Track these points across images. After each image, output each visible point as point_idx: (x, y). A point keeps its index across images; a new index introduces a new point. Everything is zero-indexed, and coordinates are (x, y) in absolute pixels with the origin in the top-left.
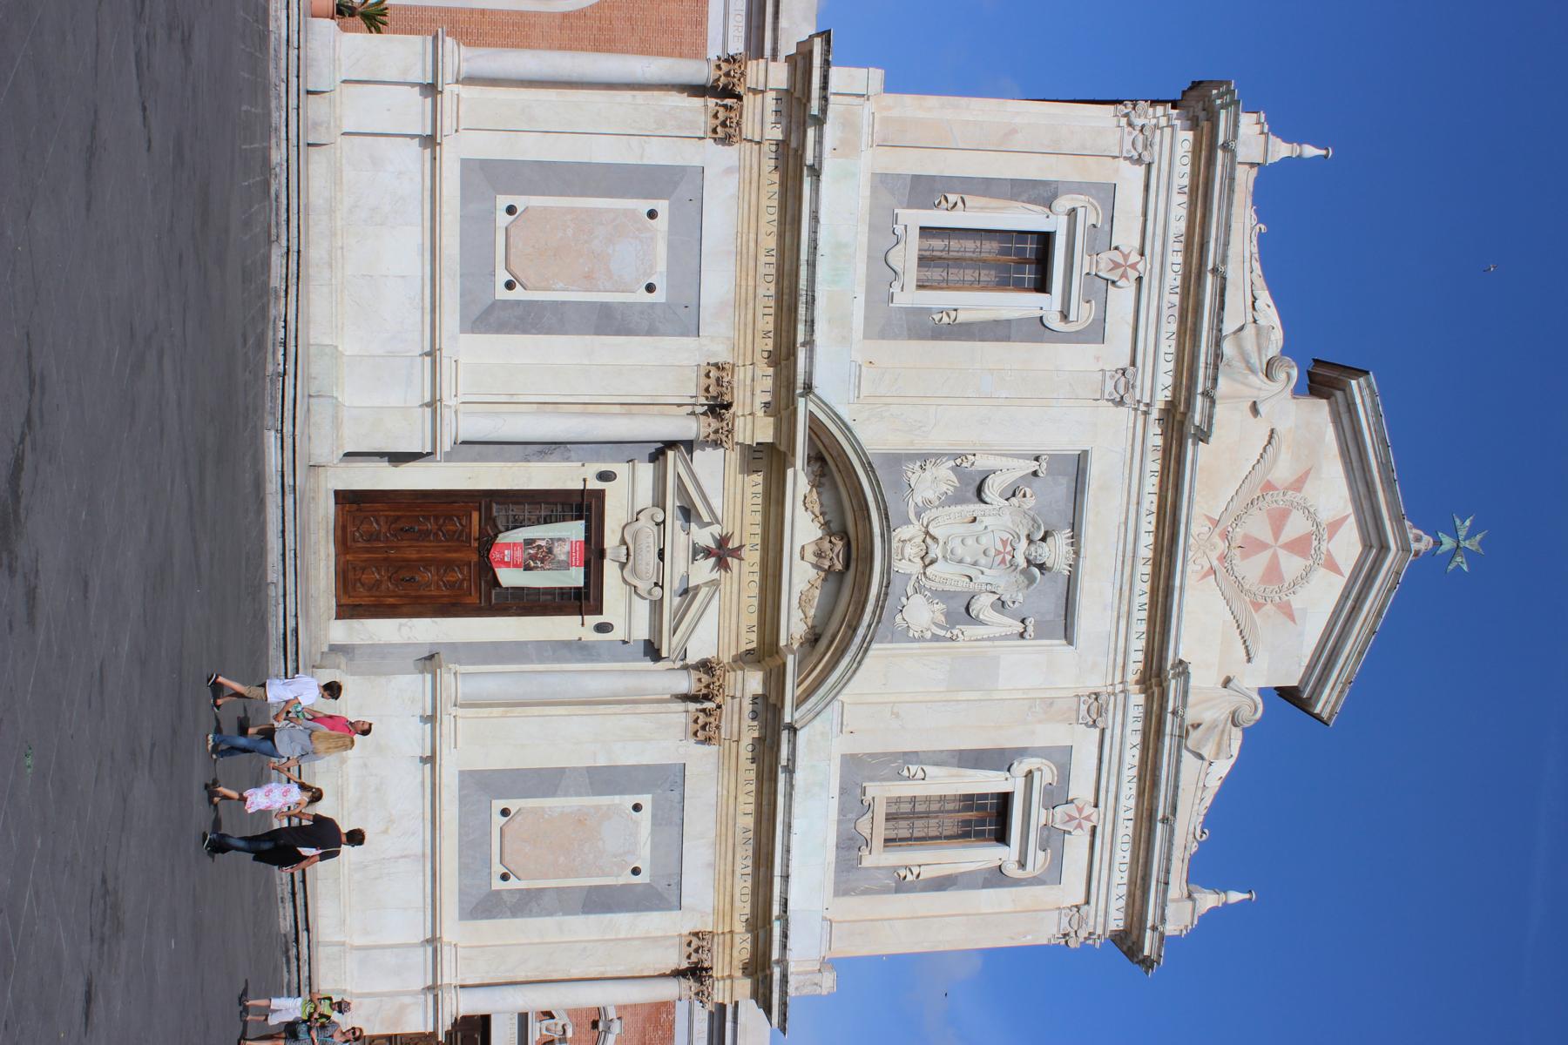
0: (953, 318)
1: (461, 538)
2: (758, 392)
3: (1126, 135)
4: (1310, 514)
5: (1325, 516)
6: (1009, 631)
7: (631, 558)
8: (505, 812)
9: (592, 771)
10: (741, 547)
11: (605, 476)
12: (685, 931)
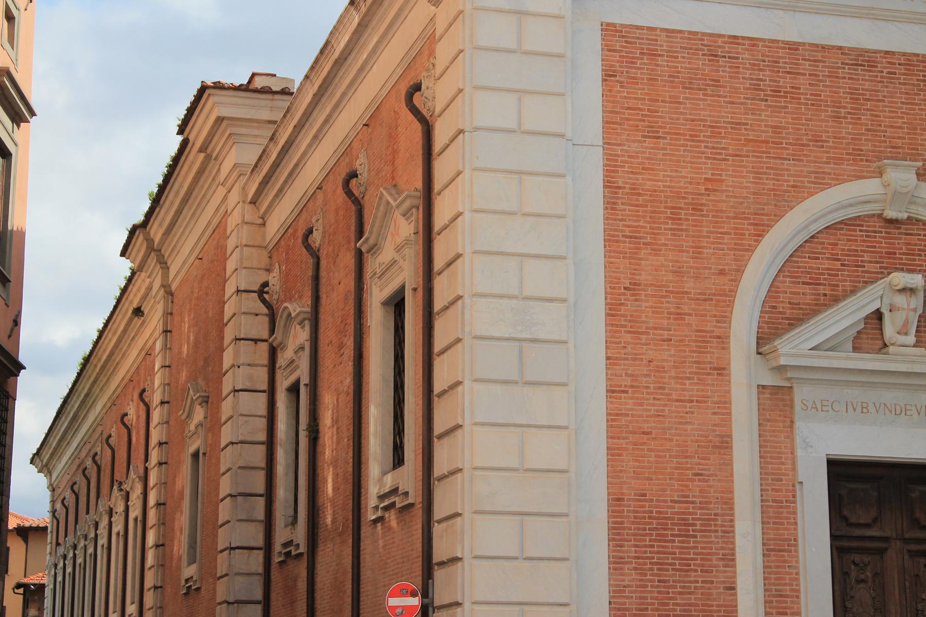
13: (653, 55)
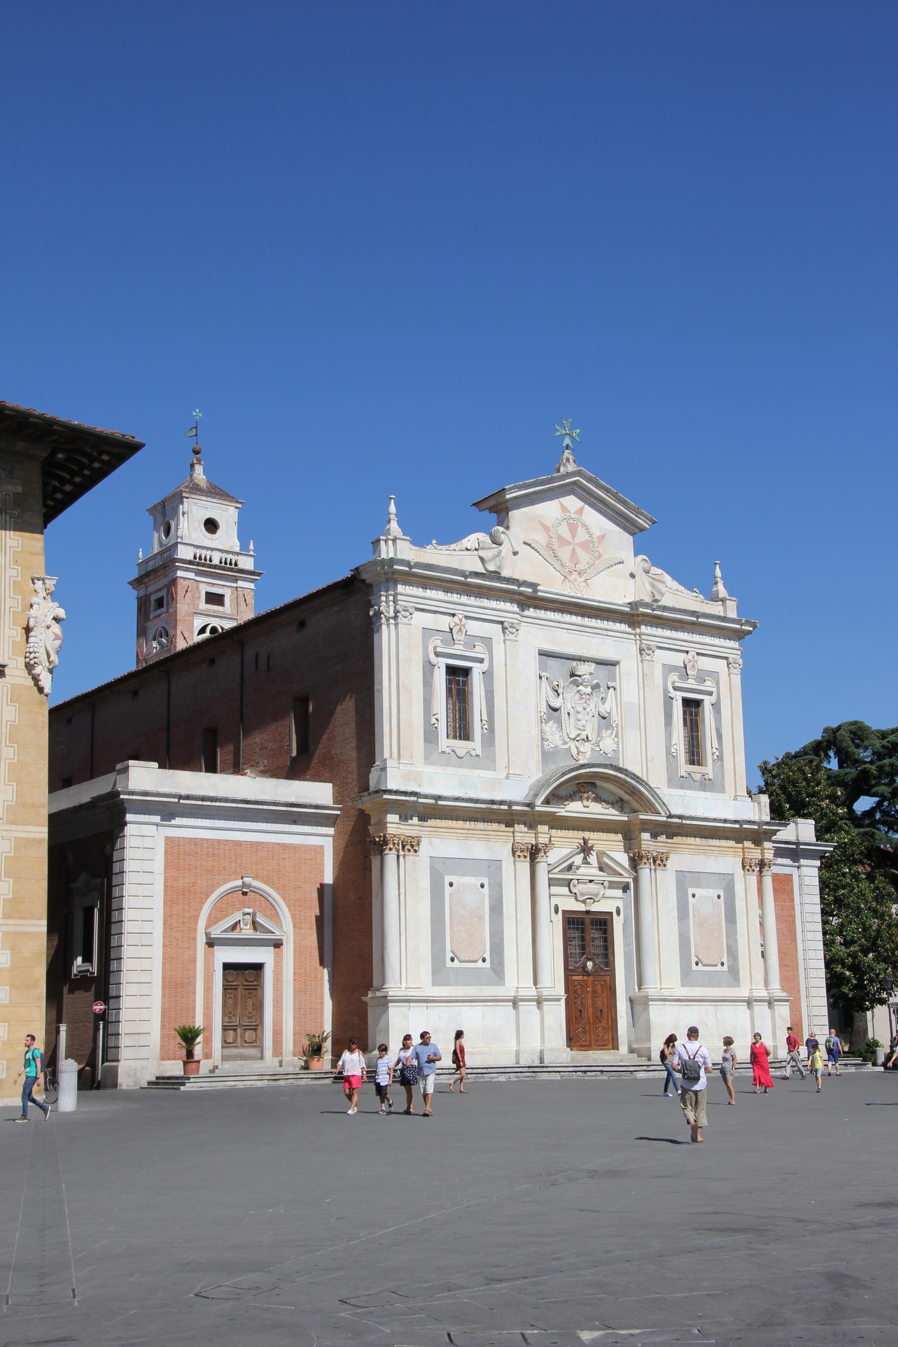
0: (486, 723)
1: (584, 984)
5: (559, 514)
6: (614, 696)
8: (697, 964)
10: (584, 839)
11: (557, 911)
12: (743, 872)
13: (179, 846)
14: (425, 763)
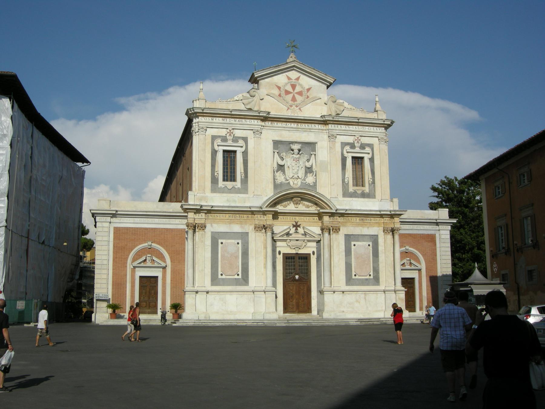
2: (261, 219)
3: (200, 133)
4: (286, 84)
5: (286, 80)
7: (298, 247)
8: (355, 275)
9: (346, 256)
10: (295, 222)
11: (280, 253)
12: (383, 234)
14: (211, 192)
